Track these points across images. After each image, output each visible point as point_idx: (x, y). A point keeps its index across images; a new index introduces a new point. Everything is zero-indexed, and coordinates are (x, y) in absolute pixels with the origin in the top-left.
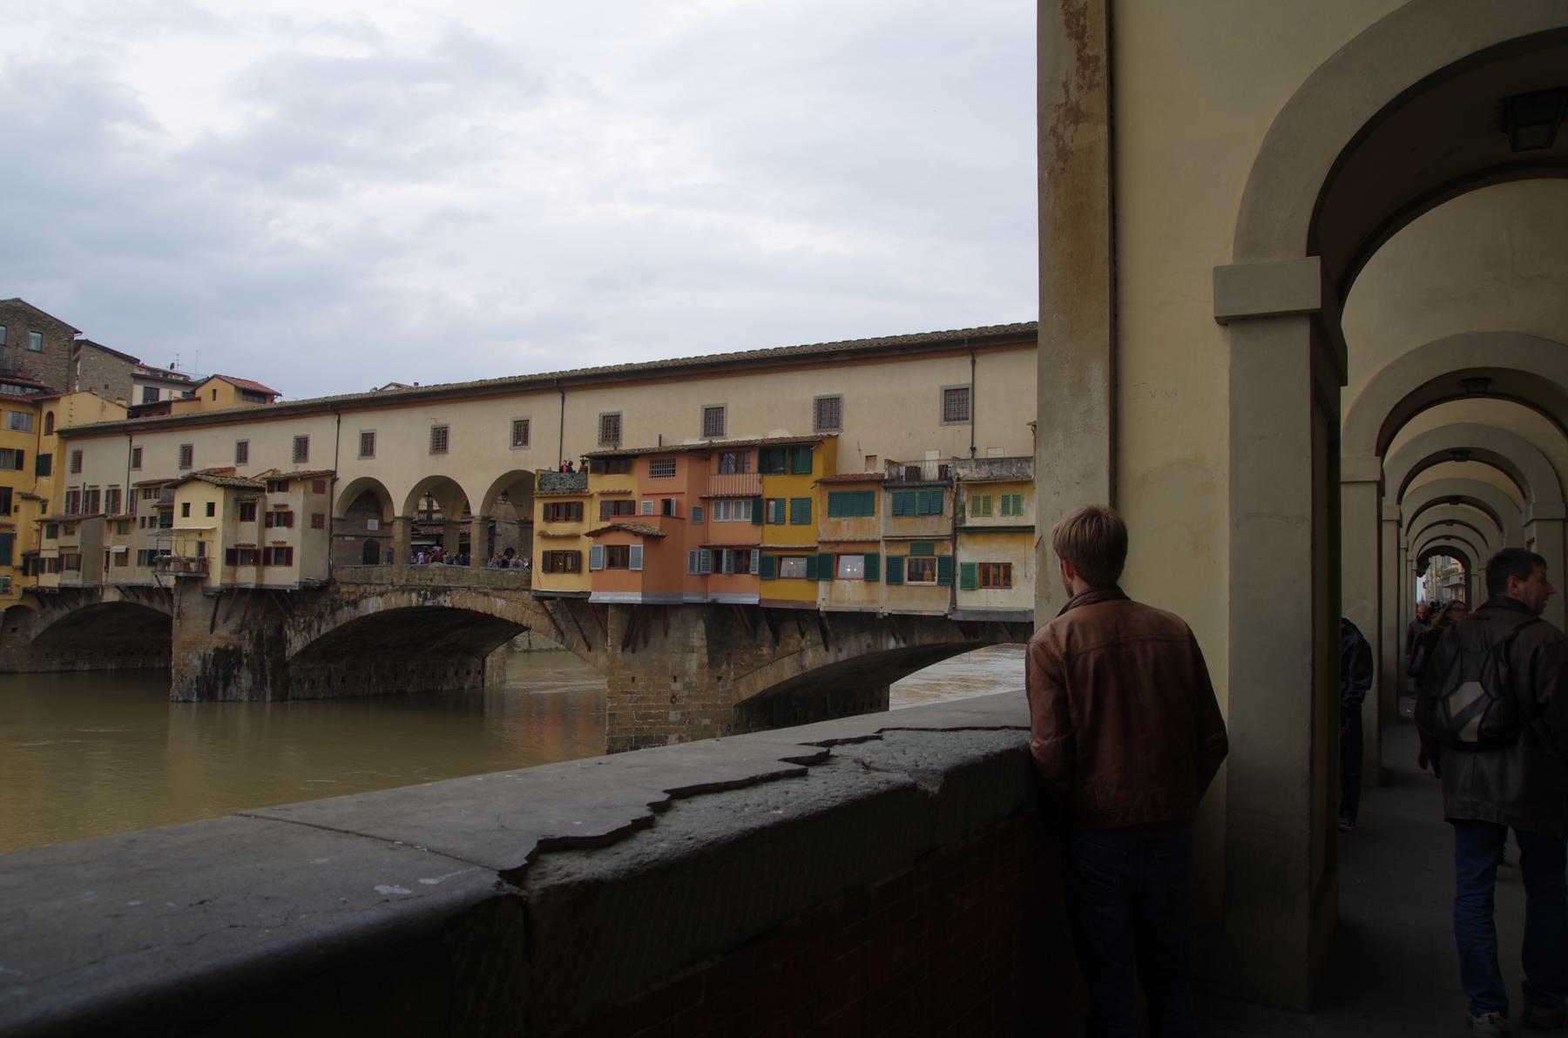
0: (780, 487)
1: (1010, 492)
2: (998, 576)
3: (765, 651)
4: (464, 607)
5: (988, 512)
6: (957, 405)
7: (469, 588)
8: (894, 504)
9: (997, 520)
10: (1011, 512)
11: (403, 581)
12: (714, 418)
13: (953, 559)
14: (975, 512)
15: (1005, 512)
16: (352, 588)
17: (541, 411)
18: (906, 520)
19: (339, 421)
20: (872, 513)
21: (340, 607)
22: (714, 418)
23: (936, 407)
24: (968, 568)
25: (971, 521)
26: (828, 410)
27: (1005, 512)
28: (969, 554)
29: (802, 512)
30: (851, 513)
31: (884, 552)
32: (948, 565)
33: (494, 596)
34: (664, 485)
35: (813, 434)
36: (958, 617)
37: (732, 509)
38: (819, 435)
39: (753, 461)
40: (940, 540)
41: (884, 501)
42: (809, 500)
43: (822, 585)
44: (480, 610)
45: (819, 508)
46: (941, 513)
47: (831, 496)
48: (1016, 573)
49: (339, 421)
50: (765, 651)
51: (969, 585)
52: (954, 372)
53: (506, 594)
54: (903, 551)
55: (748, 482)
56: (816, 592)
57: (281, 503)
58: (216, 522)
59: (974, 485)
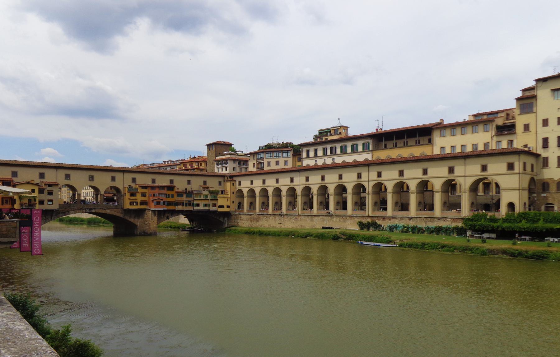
0: (170, 193)
1: (200, 195)
2: (198, 205)
3: (162, 216)
4: (99, 212)
5: (197, 197)
6: (189, 182)
7: (100, 208)
8: (186, 196)
9: (198, 198)
10: (170, 195)
11: (81, 208)
12: (154, 181)
13: (193, 203)
14: (196, 197)
15: (199, 197)
16: (63, 209)
17: (118, 176)
18: (188, 198)
19: (57, 171)
20: (183, 197)
21: (60, 213)
22: (154, 181)
23: (186, 182)
24: (195, 204)
25: (195, 198)
26: (172, 181)
27: (199, 197)
28: (195, 202)
29: (172, 196)
30: (180, 197)
31: (185, 202)
32: (193, 204)
33: (107, 210)
34: (153, 191)
35: (169, 185)
36: (194, 210)
37: (162, 196)
38: (171, 185)
39: (166, 189)
40: (192, 201)
41: (185, 196)
42: (173, 195)
43: (176, 207)
44: (103, 213)
45: (175, 196)
46: (192, 197)
47: (177, 194)
48: (200, 205)
49: (57, 171)
50: (162, 216)
51: (195, 206)
52: (189, 178)
53: (110, 209)
54: (187, 202)
55: (165, 191)
56: (175, 208)
57: (51, 190)
58: (36, 194)
59: (196, 194)
